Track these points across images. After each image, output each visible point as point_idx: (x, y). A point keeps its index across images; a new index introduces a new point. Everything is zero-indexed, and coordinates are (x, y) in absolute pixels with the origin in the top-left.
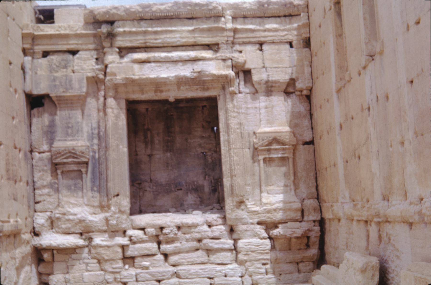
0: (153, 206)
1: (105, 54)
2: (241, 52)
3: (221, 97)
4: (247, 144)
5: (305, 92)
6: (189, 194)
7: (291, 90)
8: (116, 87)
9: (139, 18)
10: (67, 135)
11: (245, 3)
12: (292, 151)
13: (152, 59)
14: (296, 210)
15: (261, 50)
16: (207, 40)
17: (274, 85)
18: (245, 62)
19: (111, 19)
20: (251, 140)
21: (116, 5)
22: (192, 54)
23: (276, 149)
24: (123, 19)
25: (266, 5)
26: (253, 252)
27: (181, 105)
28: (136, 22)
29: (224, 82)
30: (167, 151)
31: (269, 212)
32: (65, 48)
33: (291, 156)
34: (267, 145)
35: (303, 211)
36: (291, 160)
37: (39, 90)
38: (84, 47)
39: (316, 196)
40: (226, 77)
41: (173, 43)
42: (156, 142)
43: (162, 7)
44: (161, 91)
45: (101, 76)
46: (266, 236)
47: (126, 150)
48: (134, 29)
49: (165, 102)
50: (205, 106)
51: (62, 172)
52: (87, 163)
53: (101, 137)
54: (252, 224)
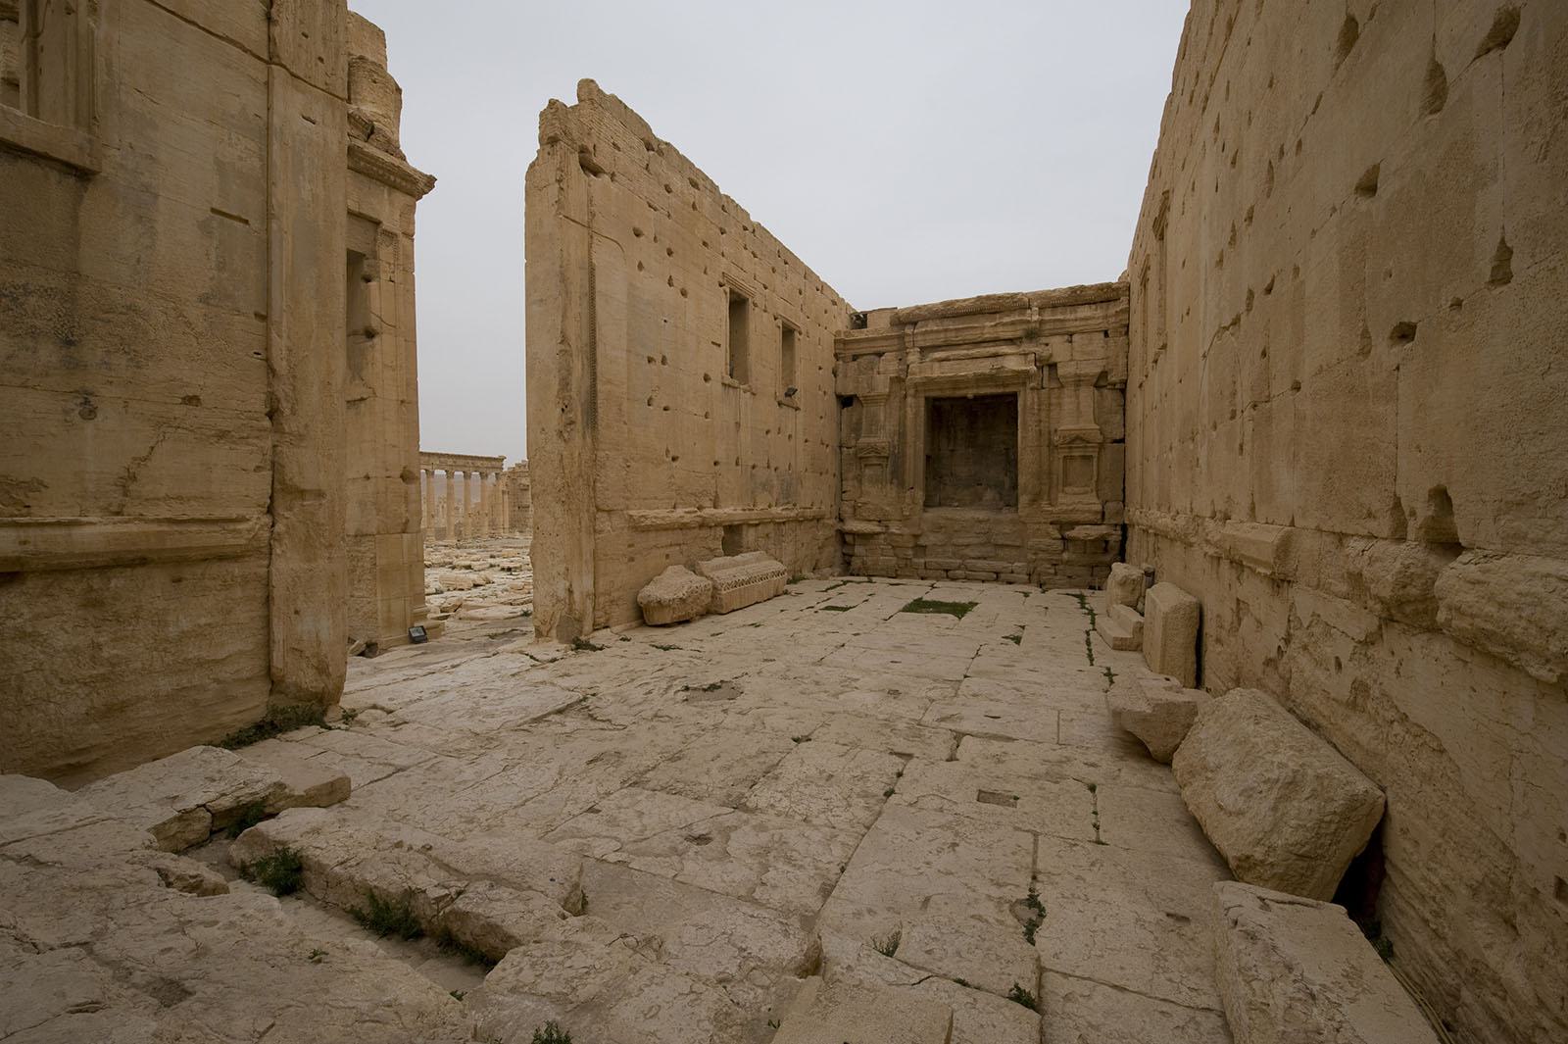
1: (907, 353)
2: (1047, 345)
4: (1047, 443)
5: (1118, 386)
7: (1102, 383)
8: (916, 385)
10: (871, 432)
12: (1097, 450)
14: (1096, 512)
15: (1071, 342)
16: (1009, 335)
18: (1051, 355)
21: (920, 304)
22: (992, 350)
24: (926, 319)
25: (1078, 292)
27: (987, 401)
28: (938, 321)
29: (1023, 377)
31: (1065, 512)
33: (1095, 455)
34: (1069, 443)
35: (1103, 514)
36: (1095, 460)
38: (889, 348)
39: (1121, 499)
40: (1027, 372)
43: (964, 304)
44: (960, 389)
47: (922, 446)
48: (936, 328)
49: (964, 398)
52: (887, 458)
53: (902, 435)
54: (1045, 523)
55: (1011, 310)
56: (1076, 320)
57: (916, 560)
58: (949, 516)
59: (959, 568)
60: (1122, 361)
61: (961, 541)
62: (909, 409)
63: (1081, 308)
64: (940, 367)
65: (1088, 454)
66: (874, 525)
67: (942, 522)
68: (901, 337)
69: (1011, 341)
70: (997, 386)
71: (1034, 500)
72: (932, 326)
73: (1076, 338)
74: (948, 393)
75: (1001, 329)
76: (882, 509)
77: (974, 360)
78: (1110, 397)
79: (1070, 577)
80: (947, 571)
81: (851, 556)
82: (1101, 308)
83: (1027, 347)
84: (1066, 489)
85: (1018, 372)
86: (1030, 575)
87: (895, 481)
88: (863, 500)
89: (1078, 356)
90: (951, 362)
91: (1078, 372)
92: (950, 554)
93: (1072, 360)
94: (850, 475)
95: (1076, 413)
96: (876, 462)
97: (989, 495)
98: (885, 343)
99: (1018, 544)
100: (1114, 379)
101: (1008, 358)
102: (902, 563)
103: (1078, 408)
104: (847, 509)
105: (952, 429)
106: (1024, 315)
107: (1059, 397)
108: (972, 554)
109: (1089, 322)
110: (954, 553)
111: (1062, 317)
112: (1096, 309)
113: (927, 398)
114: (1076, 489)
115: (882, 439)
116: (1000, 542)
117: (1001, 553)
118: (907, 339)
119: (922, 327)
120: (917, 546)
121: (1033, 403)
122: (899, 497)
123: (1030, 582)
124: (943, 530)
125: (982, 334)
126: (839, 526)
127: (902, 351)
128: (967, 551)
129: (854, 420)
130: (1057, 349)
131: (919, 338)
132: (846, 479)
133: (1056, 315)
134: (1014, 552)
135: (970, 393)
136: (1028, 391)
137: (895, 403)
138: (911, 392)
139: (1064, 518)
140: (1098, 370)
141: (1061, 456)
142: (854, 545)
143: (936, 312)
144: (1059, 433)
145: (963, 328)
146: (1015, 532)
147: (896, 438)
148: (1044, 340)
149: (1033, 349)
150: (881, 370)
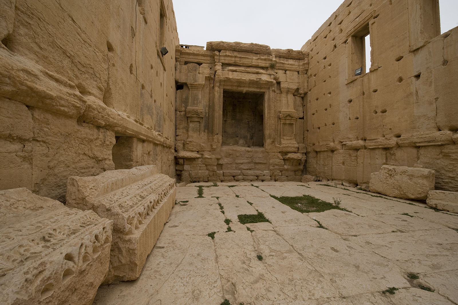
0: (225, 143)
2: (277, 73)
3: (267, 92)
5: (302, 95)
6: (241, 139)
8: (220, 81)
9: (233, 50)
11: (281, 49)
13: (238, 71)
14: (296, 147)
17: (290, 90)
19: (219, 49)
20: (278, 115)
21: (223, 41)
23: (288, 119)
24: (226, 49)
26: (276, 165)
28: (231, 52)
30: (232, 120)
31: (285, 147)
32: (196, 61)
34: (285, 117)
35: (298, 148)
37: (182, 80)
40: (272, 82)
41: (248, 64)
42: (229, 115)
44: (240, 87)
45: (213, 76)
46: (282, 158)
49: (240, 93)
50: (250, 102)
51: (190, 122)
52: (202, 118)
54: (277, 152)
55: (265, 54)
56: (288, 64)
57: (218, 172)
58: (235, 149)
59: (240, 175)
60: (306, 84)
61: (239, 161)
62: (216, 93)
63: (290, 60)
64: (232, 74)
65: (292, 123)
66: (195, 154)
67: (231, 152)
68: (213, 57)
69: (263, 68)
70: (257, 88)
71: (273, 142)
72: (228, 53)
73: (288, 72)
74: (234, 89)
75: (260, 61)
76: (200, 145)
77: (248, 74)
78: (298, 99)
79: (287, 176)
80: (234, 176)
81: (181, 171)
82: (297, 61)
83: (270, 71)
84: (284, 137)
85: (268, 82)
86: (270, 176)
87: (206, 131)
88: (189, 140)
89: (290, 80)
90: (238, 73)
91: (289, 87)
92: (234, 168)
93: (286, 81)
94: (181, 126)
95: (287, 105)
96: (197, 120)
97: (241, 141)
98: (203, 58)
99: (265, 162)
100: (301, 92)
101: (263, 75)
102: (211, 174)
103: (288, 103)
104: (180, 145)
105: (226, 111)
106: (269, 57)
107: (280, 97)
108: (244, 168)
109: (293, 66)
110: (236, 168)
111: (283, 62)
112: (295, 62)
113: (224, 89)
114: (288, 138)
115: (201, 107)
116: (257, 161)
117: (257, 167)
118: (216, 57)
119: (224, 53)
120: (218, 165)
121: (273, 98)
122: (208, 139)
123: (271, 180)
124: (231, 156)
125: (252, 62)
126: (175, 154)
127: (213, 63)
128: (242, 166)
129: (184, 97)
130: (281, 75)
131: (222, 58)
132: (179, 129)
133: (281, 61)
134: (263, 166)
135: (245, 90)
136: (271, 92)
137: (207, 91)
138: (218, 84)
139: (285, 150)
140: (296, 87)
141: (282, 123)
142: (184, 164)
143: (231, 46)
144: (282, 112)
145: (243, 57)
146: (263, 156)
147: (207, 108)
148: (276, 71)
149: (273, 73)
150: (200, 71)
